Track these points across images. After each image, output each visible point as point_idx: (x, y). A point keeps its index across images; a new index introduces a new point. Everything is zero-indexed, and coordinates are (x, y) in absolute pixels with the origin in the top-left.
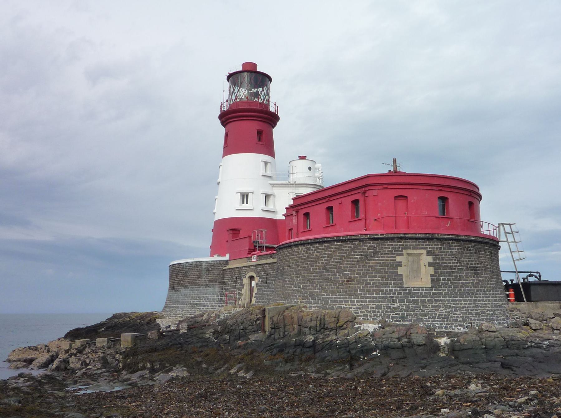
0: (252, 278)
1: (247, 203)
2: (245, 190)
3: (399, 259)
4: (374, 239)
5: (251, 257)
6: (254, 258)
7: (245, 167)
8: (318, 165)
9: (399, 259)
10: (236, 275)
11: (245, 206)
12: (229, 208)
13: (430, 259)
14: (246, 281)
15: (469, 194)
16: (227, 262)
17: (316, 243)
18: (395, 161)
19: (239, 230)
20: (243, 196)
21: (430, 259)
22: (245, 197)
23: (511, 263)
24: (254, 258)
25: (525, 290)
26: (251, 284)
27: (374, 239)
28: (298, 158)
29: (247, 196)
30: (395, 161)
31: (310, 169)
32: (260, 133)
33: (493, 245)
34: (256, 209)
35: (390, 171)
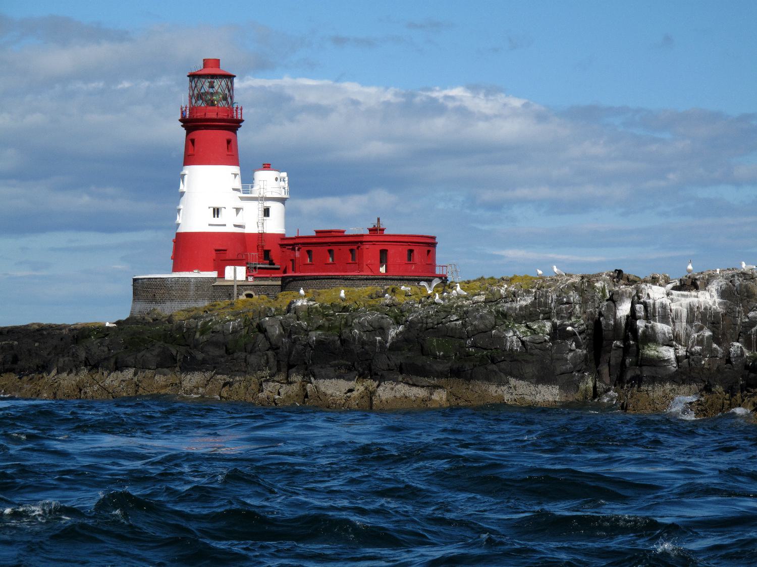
1: (218, 217)
2: (217, 205)
4: (367, 279)
11: (216, 221)
15: (429, 244)
18: (379, 219)
19: (226, 250)
20: (214, 209)
22: (216, 212)
27: (367, 279)
28: (262, 166)
29: (218, 209)
30: (379, 219)
31: (276, 179)
32: (229, 142)
34: (228, 224)
35: (375, 226)
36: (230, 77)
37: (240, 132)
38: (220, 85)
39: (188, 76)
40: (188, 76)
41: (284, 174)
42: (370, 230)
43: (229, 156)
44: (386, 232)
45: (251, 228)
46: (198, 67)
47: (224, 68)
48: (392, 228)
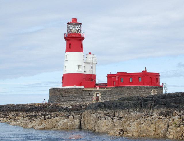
0: (97, 94)
2: (79, 64)
3: (151, 91)
5: (96, 88)
6: (98, 88)
7: (74, 55)
8: (95, 56)
9: (151, 91)
13: (156, 91)
14: (95, 94)
16: (83, 88)
17: (133, 87)
18: (146, 68)
21: (156, 91)
24: (98, 88)
26: (96, 95)
30: (146, 68)
33: (162, 88)
34: (82, 71)
36: (80, 24)
37: (84, 43)
38: (77, 27)
39: (67, 24)
40: (67, 24)
41: (95, 56)
42: (142, 71)
43: (80, 49)
44: (148, 72)
45: (88, 73)
46: (70, 21)
47: (78, 21)
48: (149, 71)
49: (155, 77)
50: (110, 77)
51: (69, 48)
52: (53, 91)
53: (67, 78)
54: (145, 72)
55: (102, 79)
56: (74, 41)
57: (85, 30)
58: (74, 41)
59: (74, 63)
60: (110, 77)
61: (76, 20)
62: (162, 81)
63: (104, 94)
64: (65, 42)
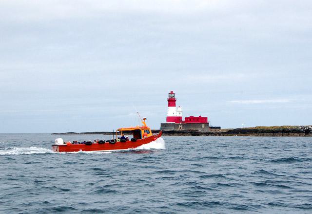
10: (178, 125)
12: (170, 115)
23: (210, 125)
25: (212, 128)
43: (174, 105)
45: (178, 116)
46: (170, 92)
47: (174, 92)
48: (202, 116)
49: (206, 119)
50: (186, 118)
51: (169, 105)
52: (163, 125)
53: (169, 119)
54: (200, 117)
55: (183, 119)
56: (172, 102)
57: (176, 97)
58: (172, 102)
59: (173, 112)
60: (186, 118)
61: (172, 92)
62: (208, 120)
63: (183, 125)
64: (167, 102)
